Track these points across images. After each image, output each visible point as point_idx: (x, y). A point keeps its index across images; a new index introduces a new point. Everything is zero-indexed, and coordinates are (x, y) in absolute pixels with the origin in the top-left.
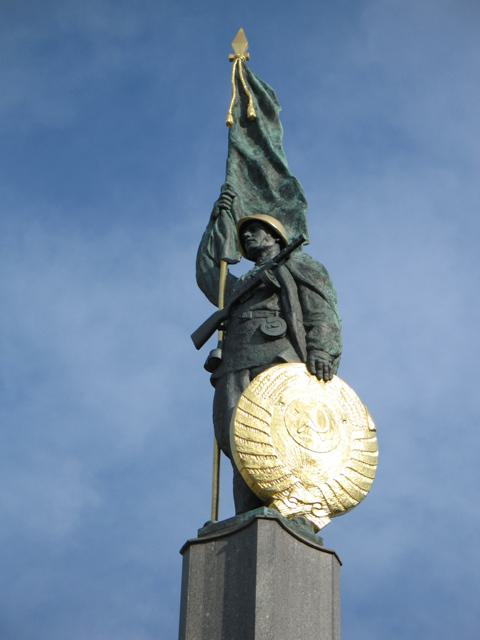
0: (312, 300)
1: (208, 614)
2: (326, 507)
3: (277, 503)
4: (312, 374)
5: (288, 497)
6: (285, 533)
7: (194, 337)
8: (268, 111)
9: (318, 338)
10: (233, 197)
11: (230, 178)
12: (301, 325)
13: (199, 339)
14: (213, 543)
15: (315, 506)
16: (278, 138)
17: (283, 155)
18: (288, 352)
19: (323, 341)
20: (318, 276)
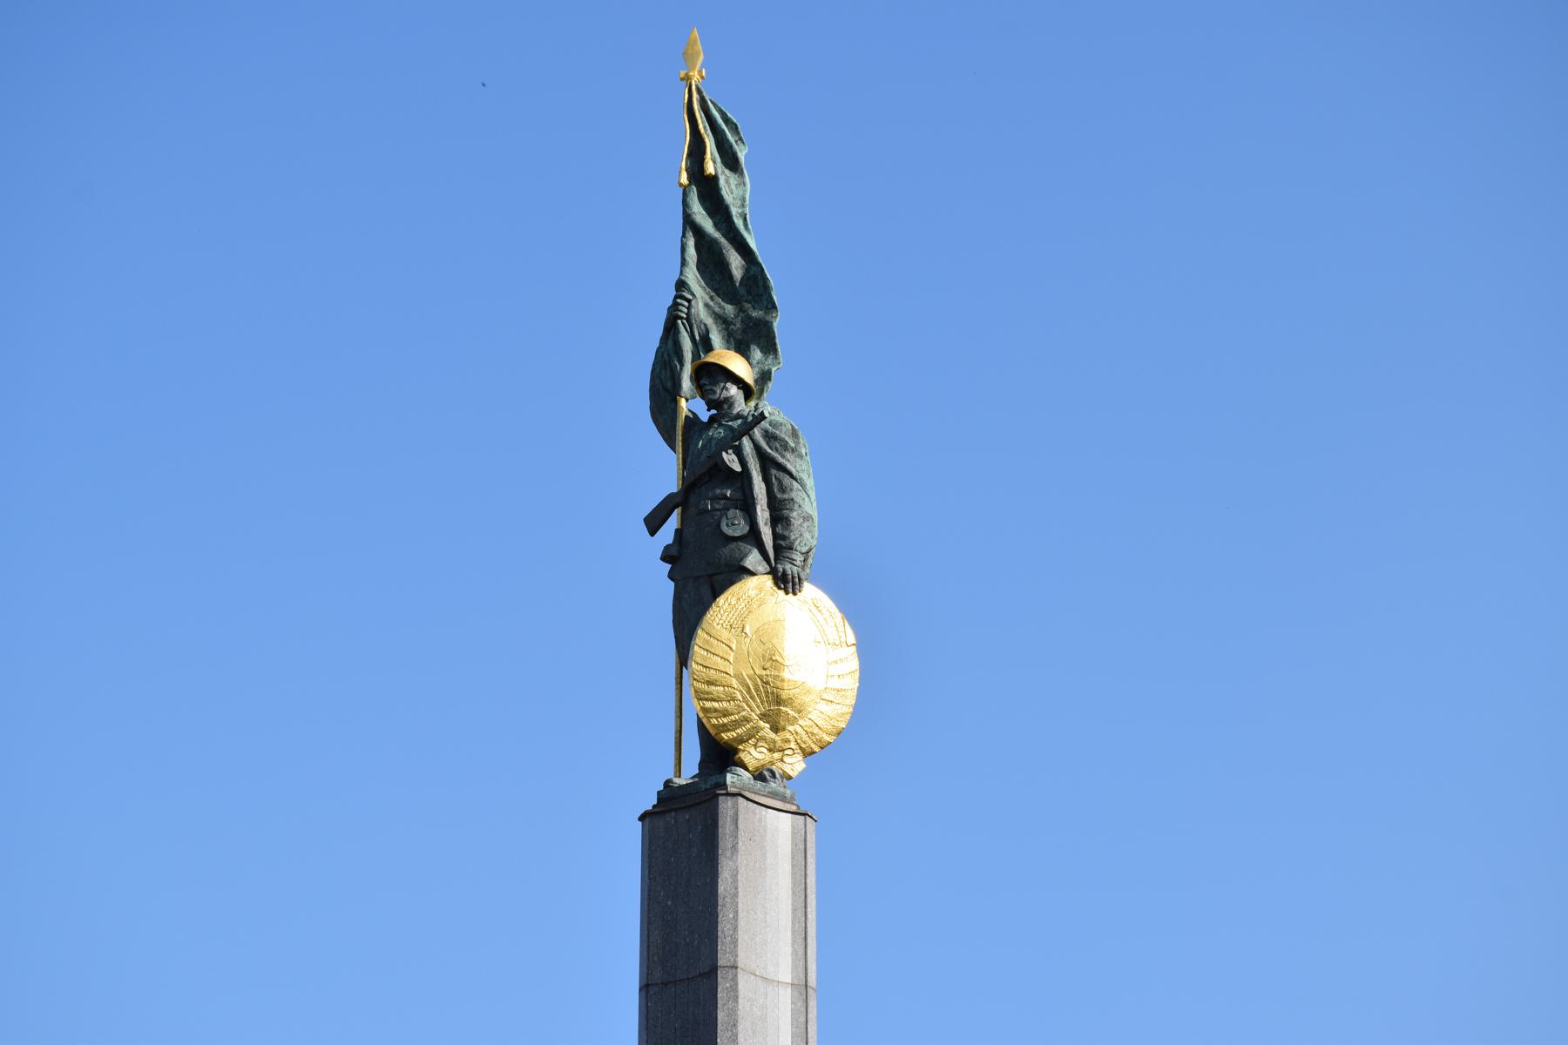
0: (780, 482)
1: (669, 903)
2: (799, 751)
3: (742, 755)
4: (780, 588)
5: (755, 746)
6: (751, 804)
7: (648, 521)
8: (730, 160)
9: (786, 533)
10: (689, 301)
11: (687, 270)
12: (767, 515)
13: (654, 522)
14: (673, 814)
15: (786, 752)
16: (743, 200)
17: (749, 233)
18: (753, 559)
19: (793, 537)
20: (785, 446)
